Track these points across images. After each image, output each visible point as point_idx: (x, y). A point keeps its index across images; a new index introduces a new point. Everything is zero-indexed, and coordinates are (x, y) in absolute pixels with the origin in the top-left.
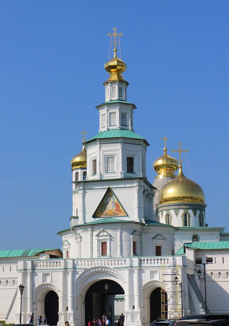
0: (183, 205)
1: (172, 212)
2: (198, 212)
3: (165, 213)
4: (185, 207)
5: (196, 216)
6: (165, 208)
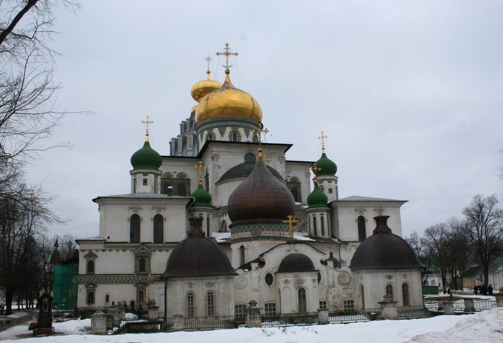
0: (230, 121)
1: (216, 131)
2: (251, 133)
3: (206, 133)
4: (233, 123)
5: (249, 137)
6: (207, 126)
